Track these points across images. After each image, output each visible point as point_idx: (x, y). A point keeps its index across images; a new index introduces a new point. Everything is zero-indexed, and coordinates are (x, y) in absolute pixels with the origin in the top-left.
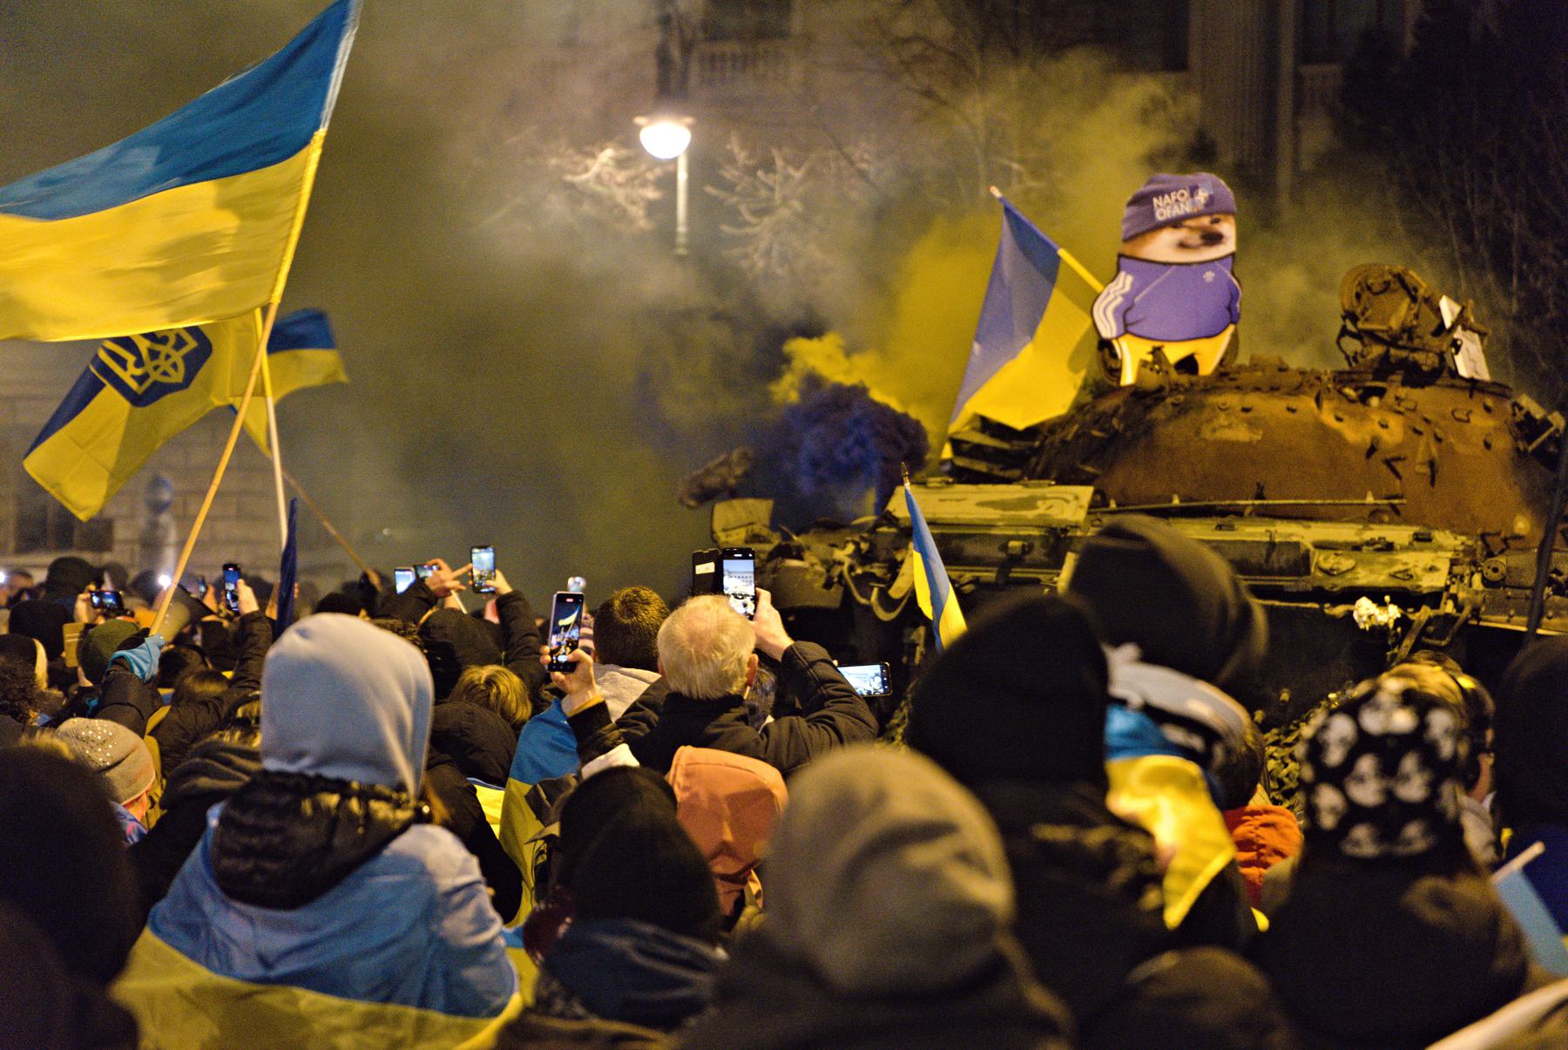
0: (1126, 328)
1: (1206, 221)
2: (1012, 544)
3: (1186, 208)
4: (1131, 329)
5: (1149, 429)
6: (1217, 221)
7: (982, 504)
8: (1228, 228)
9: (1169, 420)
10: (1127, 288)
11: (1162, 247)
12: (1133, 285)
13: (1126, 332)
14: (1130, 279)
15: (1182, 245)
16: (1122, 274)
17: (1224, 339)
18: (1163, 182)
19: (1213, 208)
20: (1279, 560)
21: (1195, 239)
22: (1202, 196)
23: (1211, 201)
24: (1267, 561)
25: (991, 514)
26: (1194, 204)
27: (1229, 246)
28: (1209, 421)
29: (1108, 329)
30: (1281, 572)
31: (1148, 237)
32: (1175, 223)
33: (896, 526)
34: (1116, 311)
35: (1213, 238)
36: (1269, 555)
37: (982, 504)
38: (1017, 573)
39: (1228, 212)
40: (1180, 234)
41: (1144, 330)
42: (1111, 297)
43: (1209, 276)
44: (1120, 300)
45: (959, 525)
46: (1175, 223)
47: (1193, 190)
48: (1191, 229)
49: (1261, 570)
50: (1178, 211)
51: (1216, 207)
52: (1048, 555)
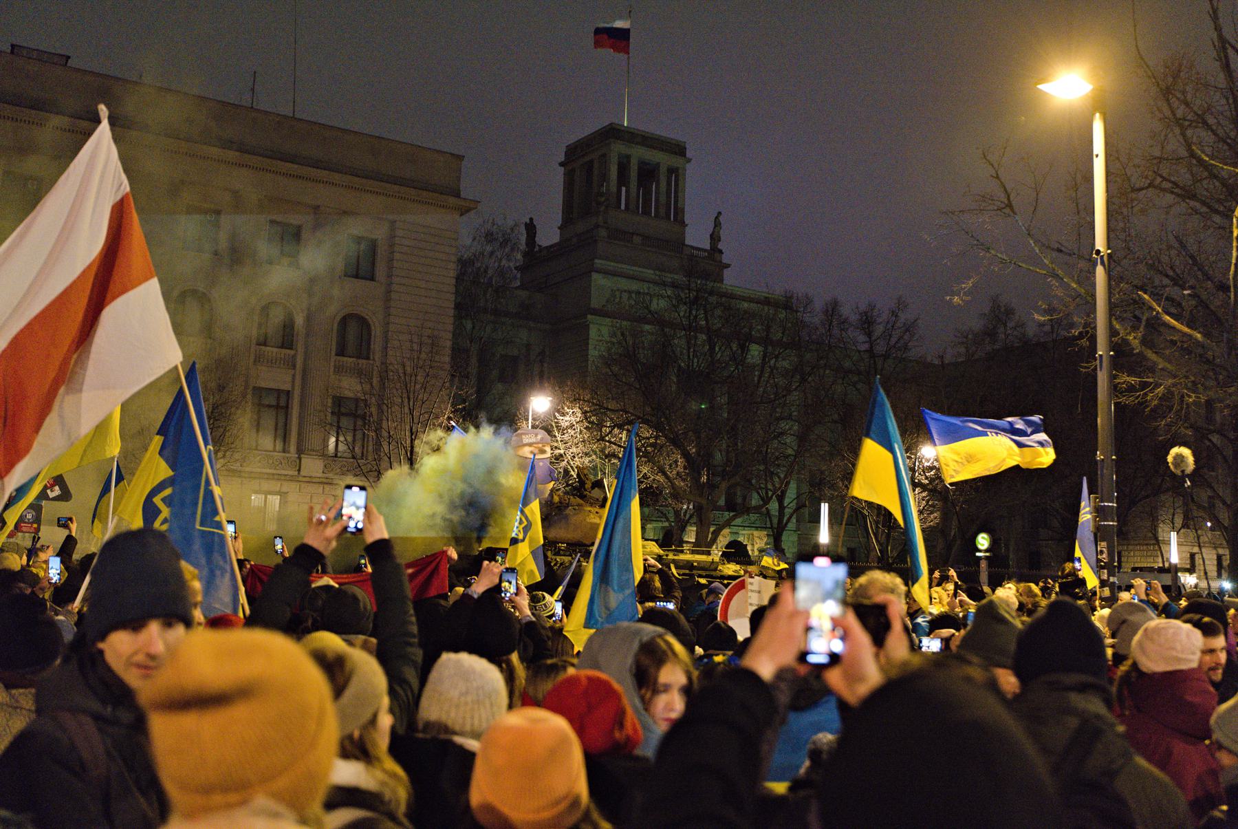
3: (533, 440)
5: (566, 517)
21: (536, 451)
22: (539, 437)
27: (548, 455)
32: (530, 445)
46: (530, 445)
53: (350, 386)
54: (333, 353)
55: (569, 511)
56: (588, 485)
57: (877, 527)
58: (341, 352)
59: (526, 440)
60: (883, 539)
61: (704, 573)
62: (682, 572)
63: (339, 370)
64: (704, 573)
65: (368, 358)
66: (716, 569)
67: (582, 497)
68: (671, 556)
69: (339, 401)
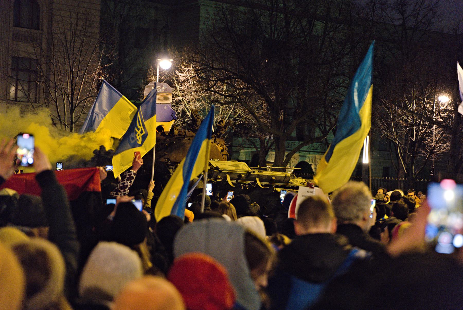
1: (165, 94)
6: (168, 95)
7: (230, 165)
17: (172, 123)
20: (286, 180)
21: (162, 98)
22: (164, 88)
23: (166, 90)
25: (233, 168)
26: (162, 90)
27: (171, 101)
35: (167, 99)
37: (230, 165)
38: (239, 181)
39: (170, 93)
43: (165, 107)
47: (162, 87)
49: (281, 182)
51: (167, 91)
53: (25, 50)
54: (12, 24)
57: (405, 152)
58: (17, 24)
60: (409, 161)
63: (17, 37)
65: (38, 29)
66: (288, 182)
68: (257, 173)
69: (16, 59)
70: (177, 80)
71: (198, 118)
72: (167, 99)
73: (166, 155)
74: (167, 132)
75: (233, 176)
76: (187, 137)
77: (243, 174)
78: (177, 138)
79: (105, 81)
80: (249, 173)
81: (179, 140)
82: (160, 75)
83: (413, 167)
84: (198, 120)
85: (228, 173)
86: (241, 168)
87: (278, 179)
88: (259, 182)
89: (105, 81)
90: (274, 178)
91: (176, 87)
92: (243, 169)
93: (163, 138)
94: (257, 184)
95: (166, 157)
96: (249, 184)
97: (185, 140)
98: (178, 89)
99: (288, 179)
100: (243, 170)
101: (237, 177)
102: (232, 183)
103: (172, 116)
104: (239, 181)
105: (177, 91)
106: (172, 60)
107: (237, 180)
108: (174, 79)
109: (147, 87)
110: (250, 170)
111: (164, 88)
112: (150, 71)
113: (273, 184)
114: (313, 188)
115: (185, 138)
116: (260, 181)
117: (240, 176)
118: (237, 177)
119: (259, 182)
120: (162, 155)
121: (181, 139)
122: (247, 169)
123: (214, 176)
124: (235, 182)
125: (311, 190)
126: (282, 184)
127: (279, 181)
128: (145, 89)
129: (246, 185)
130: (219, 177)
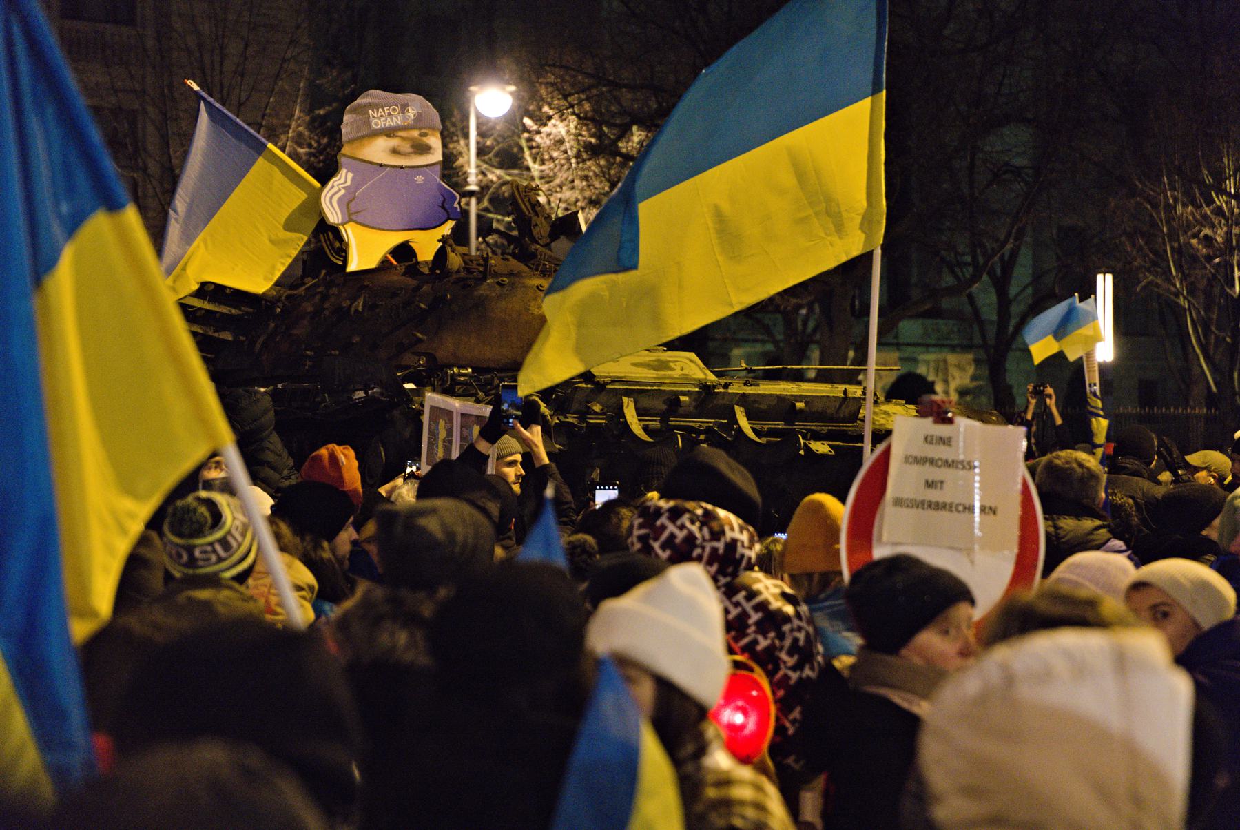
0: (350, 218)
1: (415, 133)
2: (683, 398)
4: (353, 217)
6: (425, 135)
7: (635, 365)
8: (435, 141)
9: (500, 297)
10: (349, 183)
11: (377, 151)
12: (353, 180)
13: (350, 220)
14: (350, 175)
15: (395, 152)
16: (344, 171)
18: (377, 97)
19: (419, 122)
20: (845, 411)
21: (406, 147)
22: (411, 113)
23: (419, 117)
24: (837, 411)
26: (405, 119)
27: (437, 156)
28: (535, 299)
29: (334, 216)
30: (844, 420)
31: (365, 141)
32: (389, 132)
33: (593, 383)
34: (340, 201)
35: (423, 149)
36: (840, 406)
37: (635, 365)
38: (673, 421)
39: (433, 129)
40: (394, 142)
41: (360, 219)
42: (336, 189)
43: (419, 179)
44: (343, 192)
45: (628, 383)
46: (389, 132)
47: (404, 108)
48: (403, 139)
49: (831, 419)
50: (391, 123)
52: (696, 407)
55: (487, 288)
56: (541, 229)
57: (1207, 331)
59: (379, 120)
61: (824, 428)
62: (766, 426)
64: (824, 428)
65: (131, 22)
66: (854, 417)
67: (526, 257)
68: (737, 388)
70: (531, 148)
71: (537, 214)
72: (423, 149)
73: (420, 341)
74: (426, 262)
75: (646, 402)
76: (492, 276)
77: (684, 393)
78: (460, 280)
79: (204, 94)
80: (706, 389)
81: (466, 286)
82: (482, 134)
83: (1236, 375)
84: (535, 219)
85: (628, 393)
86: (677, 373)
87: (818, 407)
88: (744, 423)
89: (204, 94)
90: (800, 405)
91: (528, 169)
92: (685, 377)
93: (411, 282)
94: (740, 430)
95: (422, 348)
96: (709, 431)
97: (484, 286)
98: (536, 174)
99: (852, 408)
100: (686, 380)
101: (664, 407)
102: (646, 429)
103: (443, 207)
104: (673, 421)
105: (533, 179)
106: (512, 88)
107: (664, 417)
108: (524, 144)
109: (354, 111)
110: (712, 377)
111: (411, 113)
112: (454, 125)
113: (799, 426)
114: (951, 421)
115: (484, 279)
116: (749, 417)
117: (673, 401)
118: (664, 407)
119: (744, 423)
120: (406, 341)
121: (472, 283)
122: (700, 376)
123: (575, 406)
124: (655, 424)
125: (943, 430)
126: (833, 427)
127: (820, 416)
128: (346, 118)
129: (699, 432)
130: (597, 408)
